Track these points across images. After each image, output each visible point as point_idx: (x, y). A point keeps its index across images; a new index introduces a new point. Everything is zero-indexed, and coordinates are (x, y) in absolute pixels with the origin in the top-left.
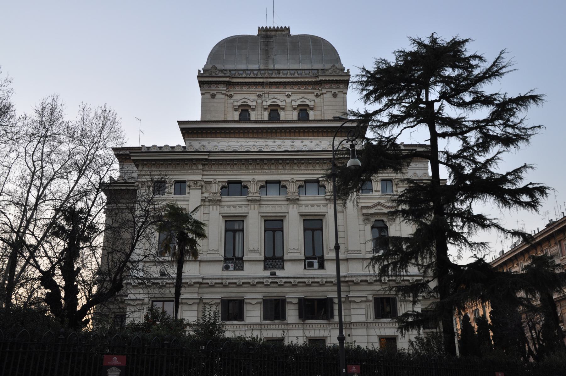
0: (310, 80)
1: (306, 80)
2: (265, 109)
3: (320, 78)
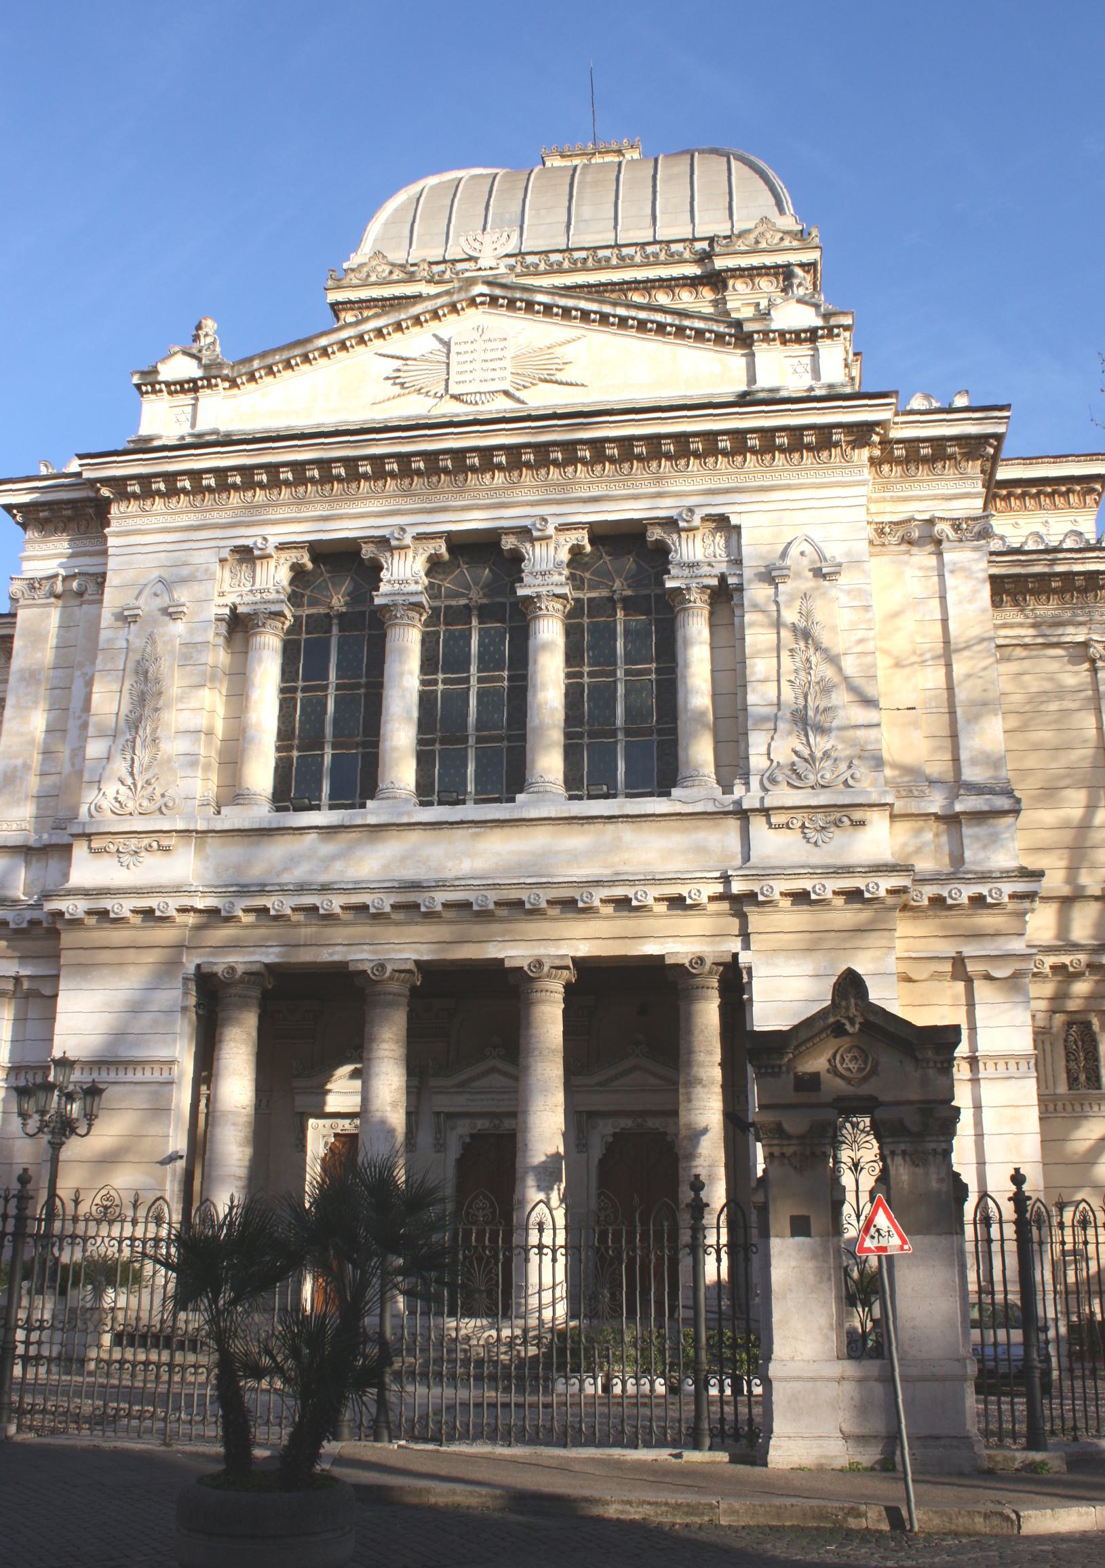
3: (720, 263)
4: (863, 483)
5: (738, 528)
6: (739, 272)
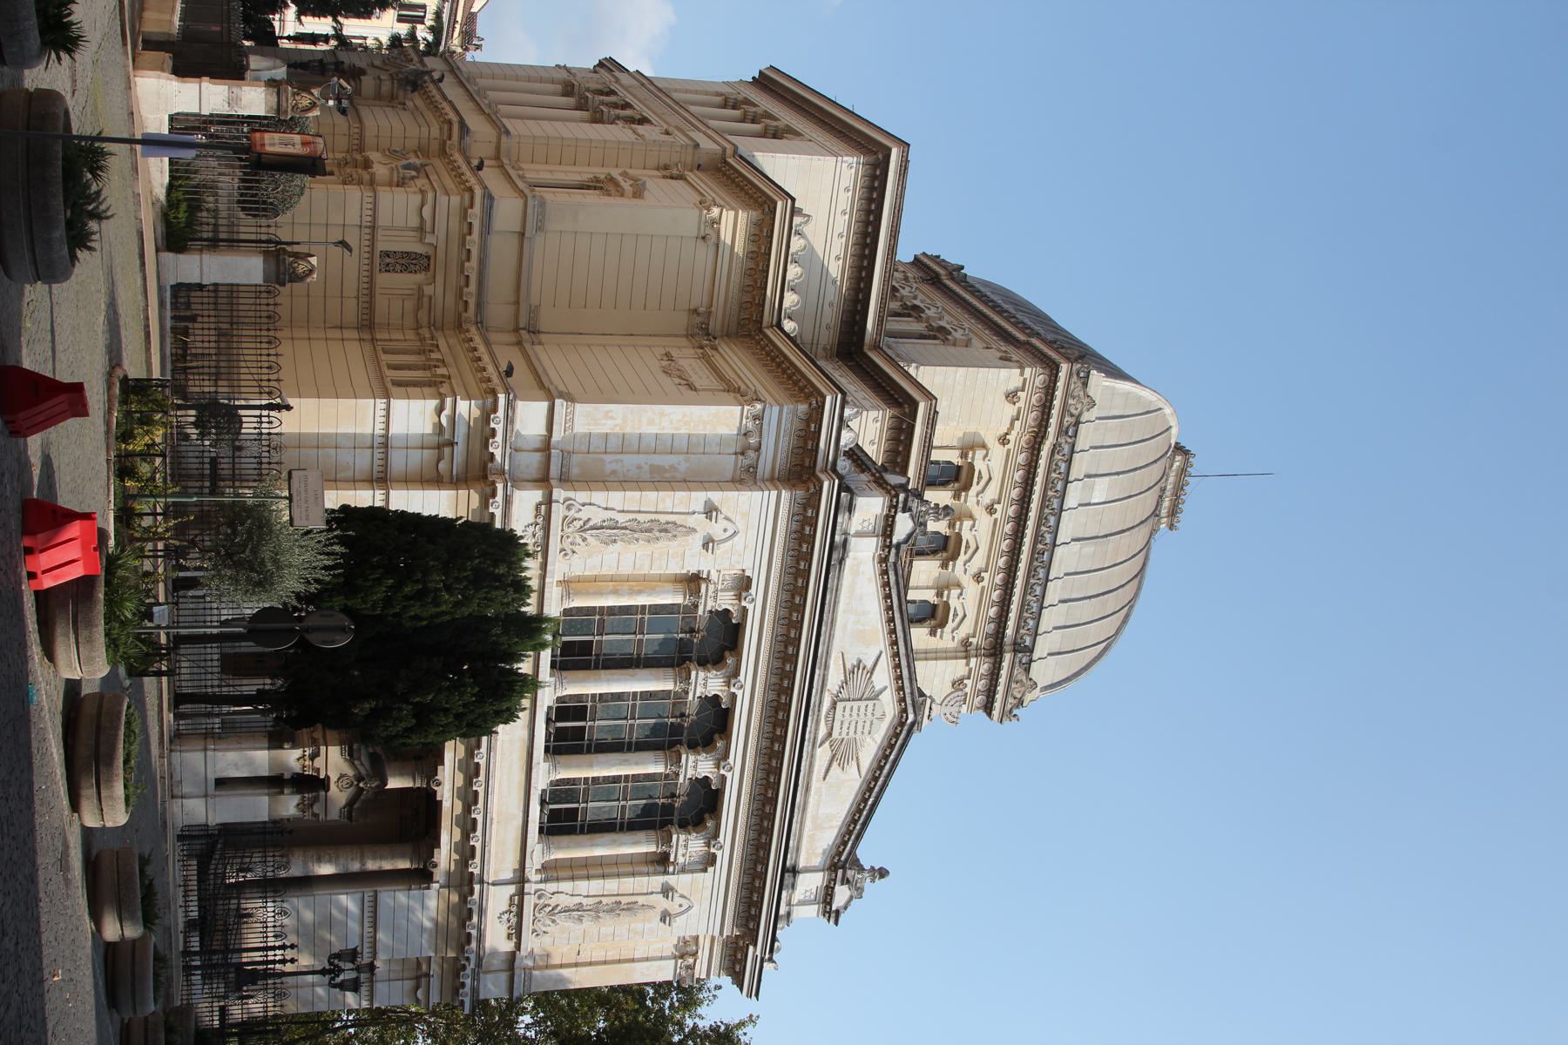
3: (1008, 657)
4: (721, 933)
5: (705, 870)
6: (994, 676)
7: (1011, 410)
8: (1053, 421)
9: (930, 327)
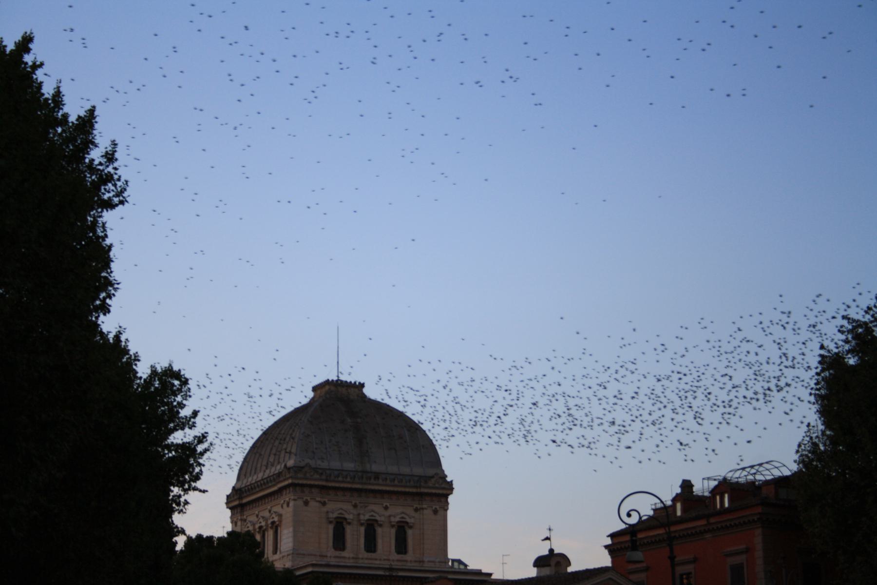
0: (411, 490)
1: (407, 490)
2: (362, 524)
3: (423, 490)
7: (312, 504)
8: (316, 483)
9: (271, 528)
